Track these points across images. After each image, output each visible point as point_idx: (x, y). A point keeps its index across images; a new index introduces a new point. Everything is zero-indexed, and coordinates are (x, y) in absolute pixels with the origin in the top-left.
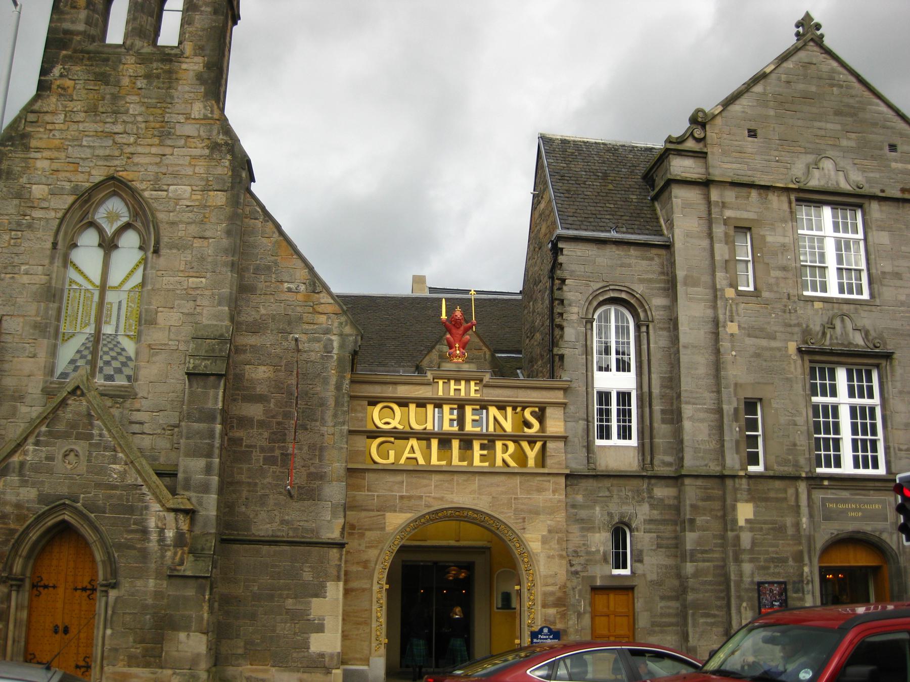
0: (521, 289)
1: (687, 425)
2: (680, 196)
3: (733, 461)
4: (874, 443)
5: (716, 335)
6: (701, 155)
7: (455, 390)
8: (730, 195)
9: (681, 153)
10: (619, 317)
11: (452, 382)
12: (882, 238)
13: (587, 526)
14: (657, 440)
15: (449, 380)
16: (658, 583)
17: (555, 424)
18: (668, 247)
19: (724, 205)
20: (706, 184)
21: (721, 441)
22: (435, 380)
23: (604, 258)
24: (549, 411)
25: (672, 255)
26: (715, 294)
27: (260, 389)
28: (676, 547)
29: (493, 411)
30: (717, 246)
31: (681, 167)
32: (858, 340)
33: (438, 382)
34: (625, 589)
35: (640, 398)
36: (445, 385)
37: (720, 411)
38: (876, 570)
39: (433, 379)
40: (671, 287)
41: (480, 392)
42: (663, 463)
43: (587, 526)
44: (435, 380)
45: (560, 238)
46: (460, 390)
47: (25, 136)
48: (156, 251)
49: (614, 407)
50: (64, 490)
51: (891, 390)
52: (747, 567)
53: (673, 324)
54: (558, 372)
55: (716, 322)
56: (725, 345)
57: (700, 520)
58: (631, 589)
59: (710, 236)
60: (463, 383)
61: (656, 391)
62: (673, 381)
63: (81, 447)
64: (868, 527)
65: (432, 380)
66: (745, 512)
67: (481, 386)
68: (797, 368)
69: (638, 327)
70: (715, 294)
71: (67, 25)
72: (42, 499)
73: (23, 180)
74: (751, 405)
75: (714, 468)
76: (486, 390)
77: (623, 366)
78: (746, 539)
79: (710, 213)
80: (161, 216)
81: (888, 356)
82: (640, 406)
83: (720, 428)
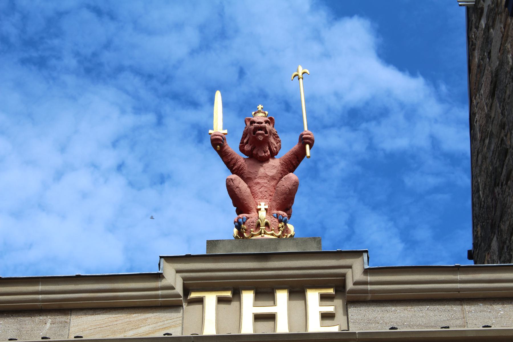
0: (470, 247)
7: (258, 318)
11: (248, 296)
15: (237, 294)
22: (193, 295)
33: (200, 301)
36: (224, 307)
39: (187, 291)
41: (340, 316)
44: (193, 295)
46: (271, 317)
60: (282, 296)
65: (179, 290)
67: (339, 302)
76: (354, 311)
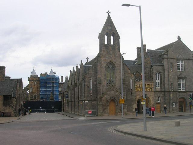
1: (166, 86)
2: (165, 60)
3: (170, 90)
4: (184, 87)
5: (169, 76)
6: (167, 55)
8: (170, 60)
9: (165, 55)
10: (158, 74)
12: (186, 64)
13: (156, 97)
14: (163, 87)
16: (163, 103)
17: (153, 86)
18: (163, 66)
19: (170, 61)
20: (168, 58)
21: (169, 88)
23: (157, 67)
24: (152, 85)
25: (164, 67)
26: (169, 72)
27: (127, 84)
28: (164, 99)
29: (146, 85)
30: (169, 66)
31: (165, 56)
32: (183, 76)
34: (159, 103)
35: (160, 83)
37: (169, 84)
38: (184, 101)
40: (164, 70)
42: (163, 90)
43: (156, 97)
45: (152, 65)
47: (100, 56)
48: (116, 70)
49: (158, 84)
50: (112, 96)
51: (186, 81)
52: (172, 101)
53: (164, 75)
54: (152, 80)
55: (169, 75)
56: (170, 77)
57: (167, 96)
58: (160, 103)
59: (168, 64)
61: (162, 82)
62: (164, 81)
63: (113, 92)
64: (183, 97)
66: (171, 95)
68: (177, 79)
69: (160, 75)
70: (169, 72)
71: (102, 42)
72: (110, 97)
73: (101, 62)
74: (172, 84)
75: (168, 90)
77: (159, 79)
78: (172, 98)
79: (168, 62)
80: (116, 66)
81: (186, 78)
82: (160, 84)
83: (169, 86)
